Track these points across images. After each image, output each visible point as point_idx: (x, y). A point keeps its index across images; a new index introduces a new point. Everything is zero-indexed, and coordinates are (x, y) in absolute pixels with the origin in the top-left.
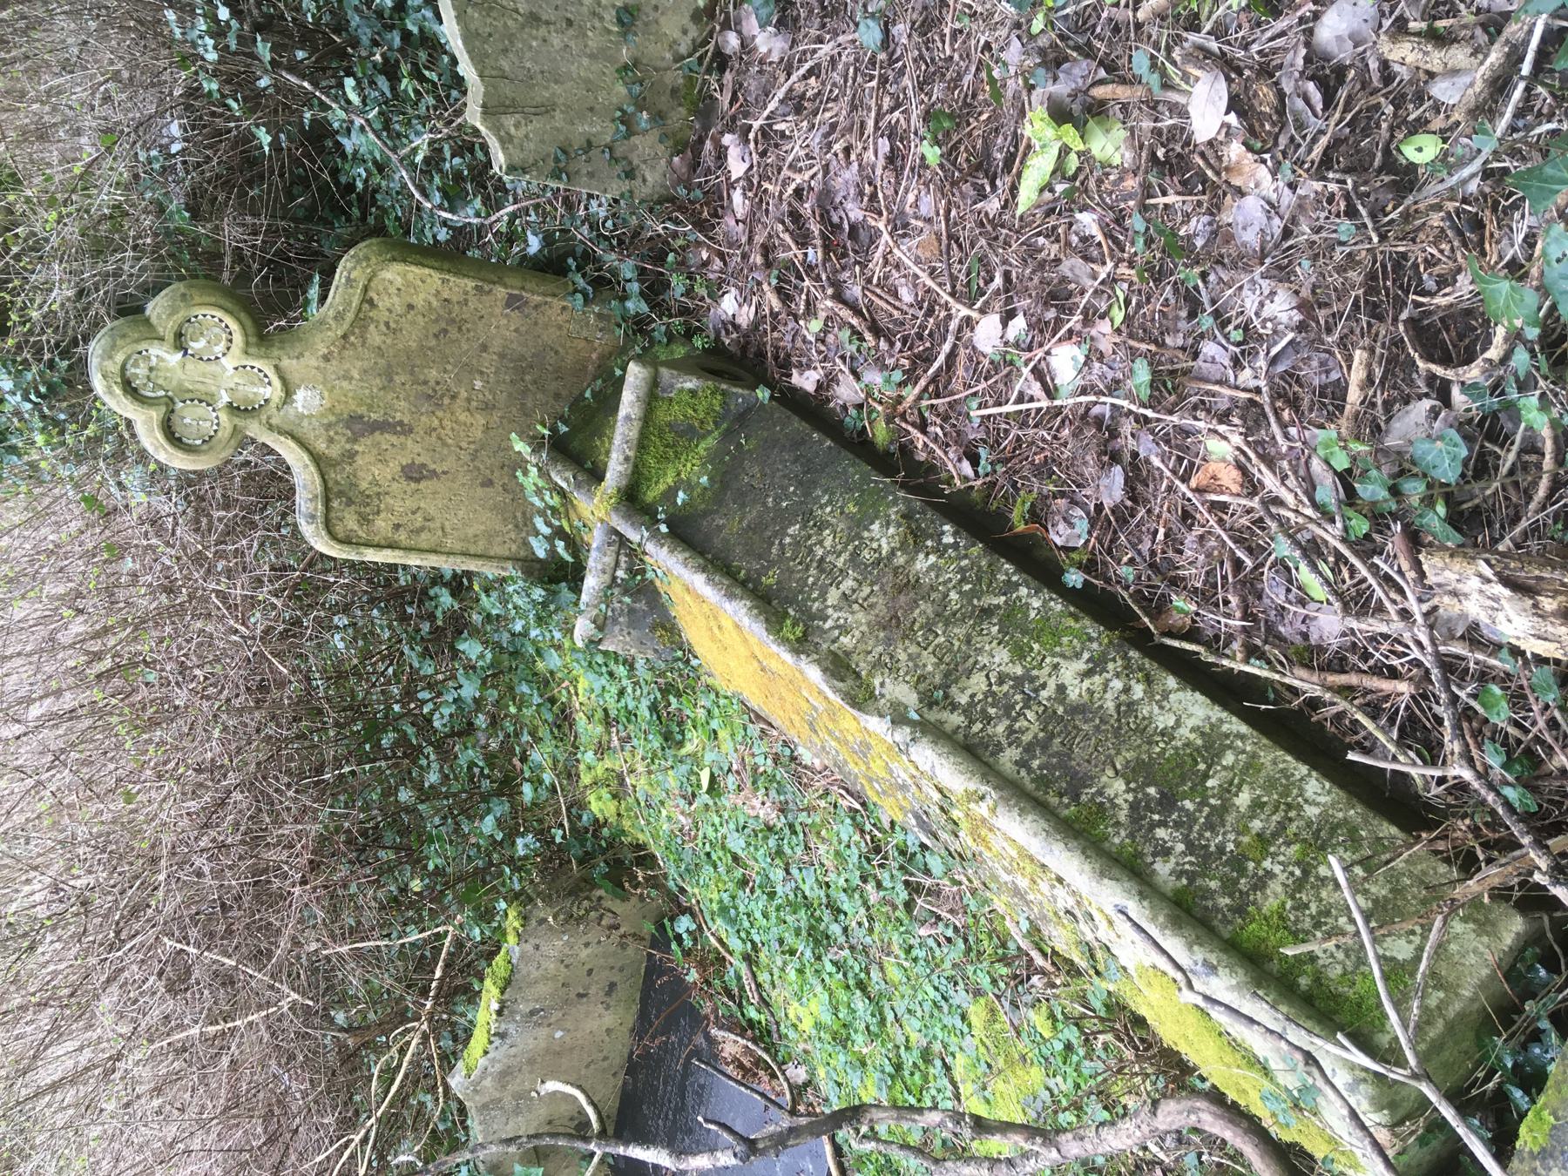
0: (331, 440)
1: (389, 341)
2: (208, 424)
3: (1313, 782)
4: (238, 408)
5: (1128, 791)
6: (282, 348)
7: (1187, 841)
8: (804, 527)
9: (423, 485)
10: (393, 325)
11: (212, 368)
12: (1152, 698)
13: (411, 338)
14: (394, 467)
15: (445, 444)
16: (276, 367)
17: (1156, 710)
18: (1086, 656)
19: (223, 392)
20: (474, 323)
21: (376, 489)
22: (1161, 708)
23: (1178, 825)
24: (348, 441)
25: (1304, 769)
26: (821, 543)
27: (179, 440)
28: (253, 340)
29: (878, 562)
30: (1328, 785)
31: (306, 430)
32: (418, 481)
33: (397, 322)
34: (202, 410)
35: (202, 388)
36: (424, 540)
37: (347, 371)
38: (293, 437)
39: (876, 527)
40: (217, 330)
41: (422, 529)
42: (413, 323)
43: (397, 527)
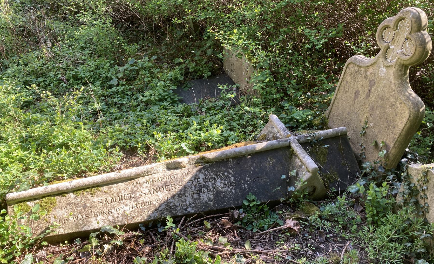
0: (371, 74)
1: (390, 103)
2: (386, 39)
3: (62, 232)
4: (388, 50)
5: (93, 201)
6: (398, 70)
7: (74, 203)
8: (230, 181)
9: (354, 95)
10: (393, 107)
11: (400, 47)
12: (106, 219)
13: (389, 110)
14: (360, 89)
15: (361, 106)
16: (393, 66)
17: (103, 218)
18: (129, 215)
19: (393, 47)
20: (387, 133)
21: (356, 81)
22: (103, 219)
23: (78, 204)
24: (370, 78)
25: (66, 232)
26: (221, 182)
27: (385, 29)
28: (402, 62)
29: (200, 191)
30: (60, 233)
31: (375, 66)
32: (355, 94)
33: (394, 108)
34: (391, 39)
35: (396, 41)
36: (342, 88)
37: (386, 87)
38: (375, 63)
39: (212, 197)
40: (409, 52)
41: (344, 89)
42: (392, 114)
43: (347, 82)
